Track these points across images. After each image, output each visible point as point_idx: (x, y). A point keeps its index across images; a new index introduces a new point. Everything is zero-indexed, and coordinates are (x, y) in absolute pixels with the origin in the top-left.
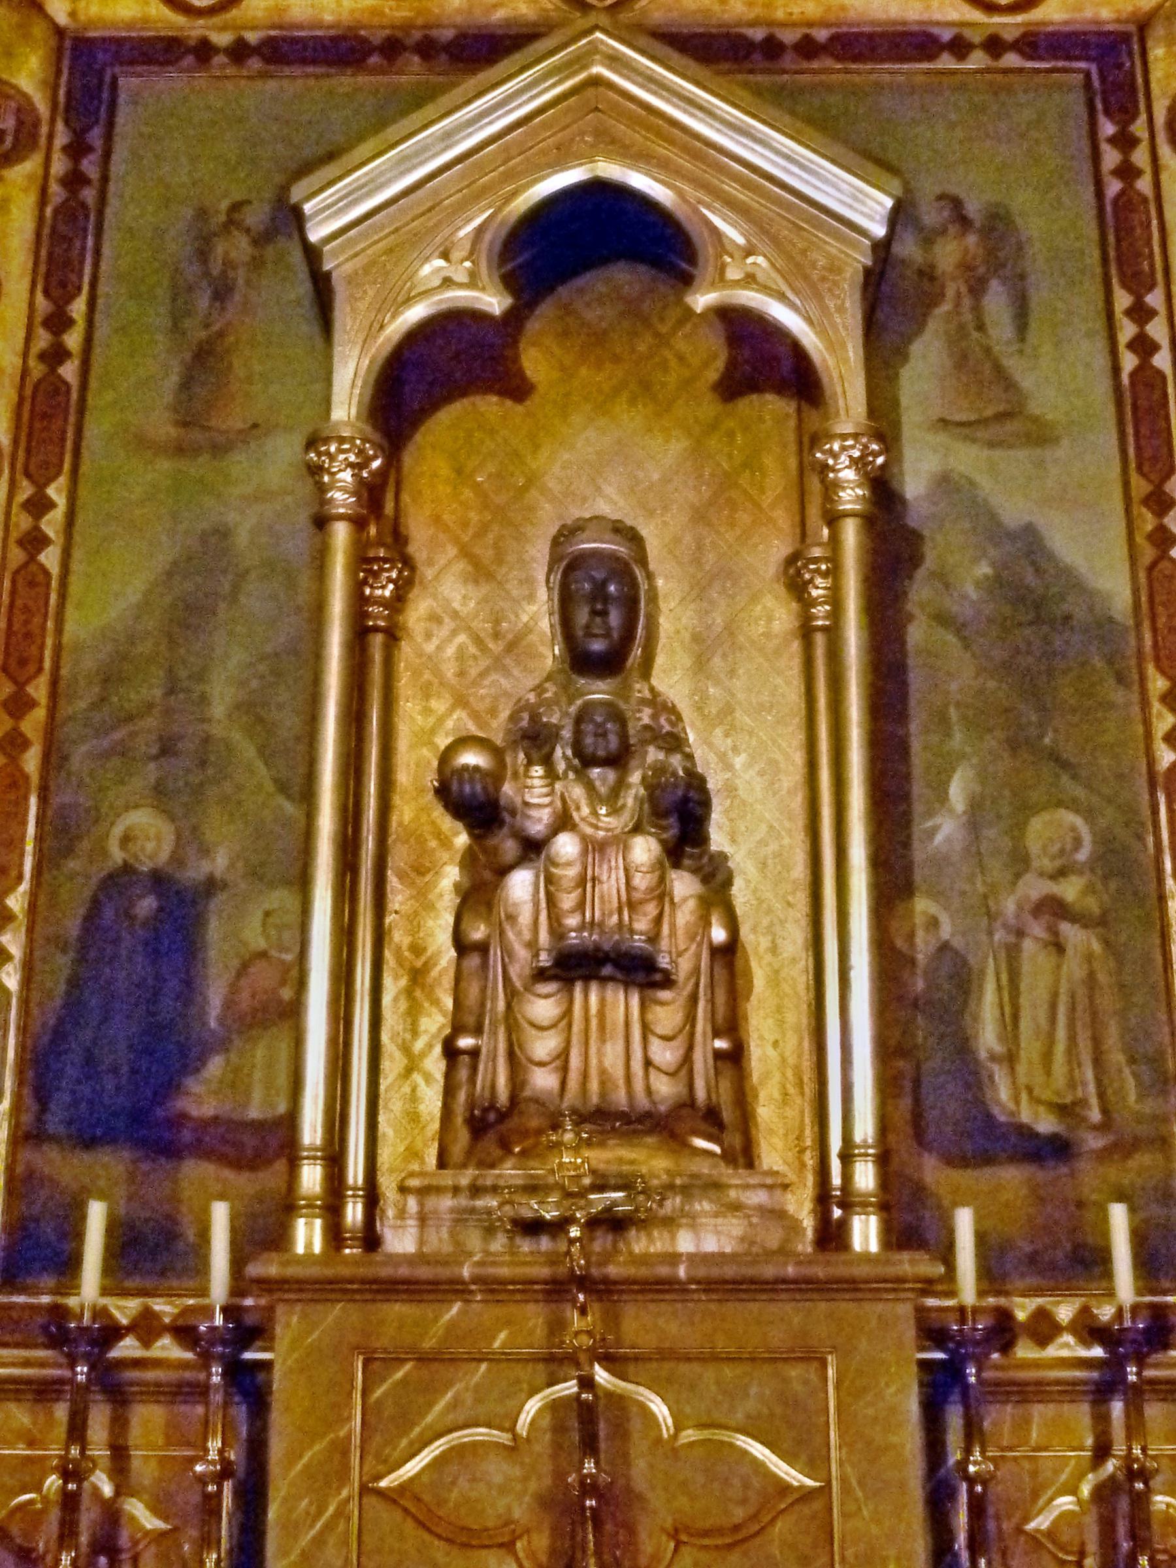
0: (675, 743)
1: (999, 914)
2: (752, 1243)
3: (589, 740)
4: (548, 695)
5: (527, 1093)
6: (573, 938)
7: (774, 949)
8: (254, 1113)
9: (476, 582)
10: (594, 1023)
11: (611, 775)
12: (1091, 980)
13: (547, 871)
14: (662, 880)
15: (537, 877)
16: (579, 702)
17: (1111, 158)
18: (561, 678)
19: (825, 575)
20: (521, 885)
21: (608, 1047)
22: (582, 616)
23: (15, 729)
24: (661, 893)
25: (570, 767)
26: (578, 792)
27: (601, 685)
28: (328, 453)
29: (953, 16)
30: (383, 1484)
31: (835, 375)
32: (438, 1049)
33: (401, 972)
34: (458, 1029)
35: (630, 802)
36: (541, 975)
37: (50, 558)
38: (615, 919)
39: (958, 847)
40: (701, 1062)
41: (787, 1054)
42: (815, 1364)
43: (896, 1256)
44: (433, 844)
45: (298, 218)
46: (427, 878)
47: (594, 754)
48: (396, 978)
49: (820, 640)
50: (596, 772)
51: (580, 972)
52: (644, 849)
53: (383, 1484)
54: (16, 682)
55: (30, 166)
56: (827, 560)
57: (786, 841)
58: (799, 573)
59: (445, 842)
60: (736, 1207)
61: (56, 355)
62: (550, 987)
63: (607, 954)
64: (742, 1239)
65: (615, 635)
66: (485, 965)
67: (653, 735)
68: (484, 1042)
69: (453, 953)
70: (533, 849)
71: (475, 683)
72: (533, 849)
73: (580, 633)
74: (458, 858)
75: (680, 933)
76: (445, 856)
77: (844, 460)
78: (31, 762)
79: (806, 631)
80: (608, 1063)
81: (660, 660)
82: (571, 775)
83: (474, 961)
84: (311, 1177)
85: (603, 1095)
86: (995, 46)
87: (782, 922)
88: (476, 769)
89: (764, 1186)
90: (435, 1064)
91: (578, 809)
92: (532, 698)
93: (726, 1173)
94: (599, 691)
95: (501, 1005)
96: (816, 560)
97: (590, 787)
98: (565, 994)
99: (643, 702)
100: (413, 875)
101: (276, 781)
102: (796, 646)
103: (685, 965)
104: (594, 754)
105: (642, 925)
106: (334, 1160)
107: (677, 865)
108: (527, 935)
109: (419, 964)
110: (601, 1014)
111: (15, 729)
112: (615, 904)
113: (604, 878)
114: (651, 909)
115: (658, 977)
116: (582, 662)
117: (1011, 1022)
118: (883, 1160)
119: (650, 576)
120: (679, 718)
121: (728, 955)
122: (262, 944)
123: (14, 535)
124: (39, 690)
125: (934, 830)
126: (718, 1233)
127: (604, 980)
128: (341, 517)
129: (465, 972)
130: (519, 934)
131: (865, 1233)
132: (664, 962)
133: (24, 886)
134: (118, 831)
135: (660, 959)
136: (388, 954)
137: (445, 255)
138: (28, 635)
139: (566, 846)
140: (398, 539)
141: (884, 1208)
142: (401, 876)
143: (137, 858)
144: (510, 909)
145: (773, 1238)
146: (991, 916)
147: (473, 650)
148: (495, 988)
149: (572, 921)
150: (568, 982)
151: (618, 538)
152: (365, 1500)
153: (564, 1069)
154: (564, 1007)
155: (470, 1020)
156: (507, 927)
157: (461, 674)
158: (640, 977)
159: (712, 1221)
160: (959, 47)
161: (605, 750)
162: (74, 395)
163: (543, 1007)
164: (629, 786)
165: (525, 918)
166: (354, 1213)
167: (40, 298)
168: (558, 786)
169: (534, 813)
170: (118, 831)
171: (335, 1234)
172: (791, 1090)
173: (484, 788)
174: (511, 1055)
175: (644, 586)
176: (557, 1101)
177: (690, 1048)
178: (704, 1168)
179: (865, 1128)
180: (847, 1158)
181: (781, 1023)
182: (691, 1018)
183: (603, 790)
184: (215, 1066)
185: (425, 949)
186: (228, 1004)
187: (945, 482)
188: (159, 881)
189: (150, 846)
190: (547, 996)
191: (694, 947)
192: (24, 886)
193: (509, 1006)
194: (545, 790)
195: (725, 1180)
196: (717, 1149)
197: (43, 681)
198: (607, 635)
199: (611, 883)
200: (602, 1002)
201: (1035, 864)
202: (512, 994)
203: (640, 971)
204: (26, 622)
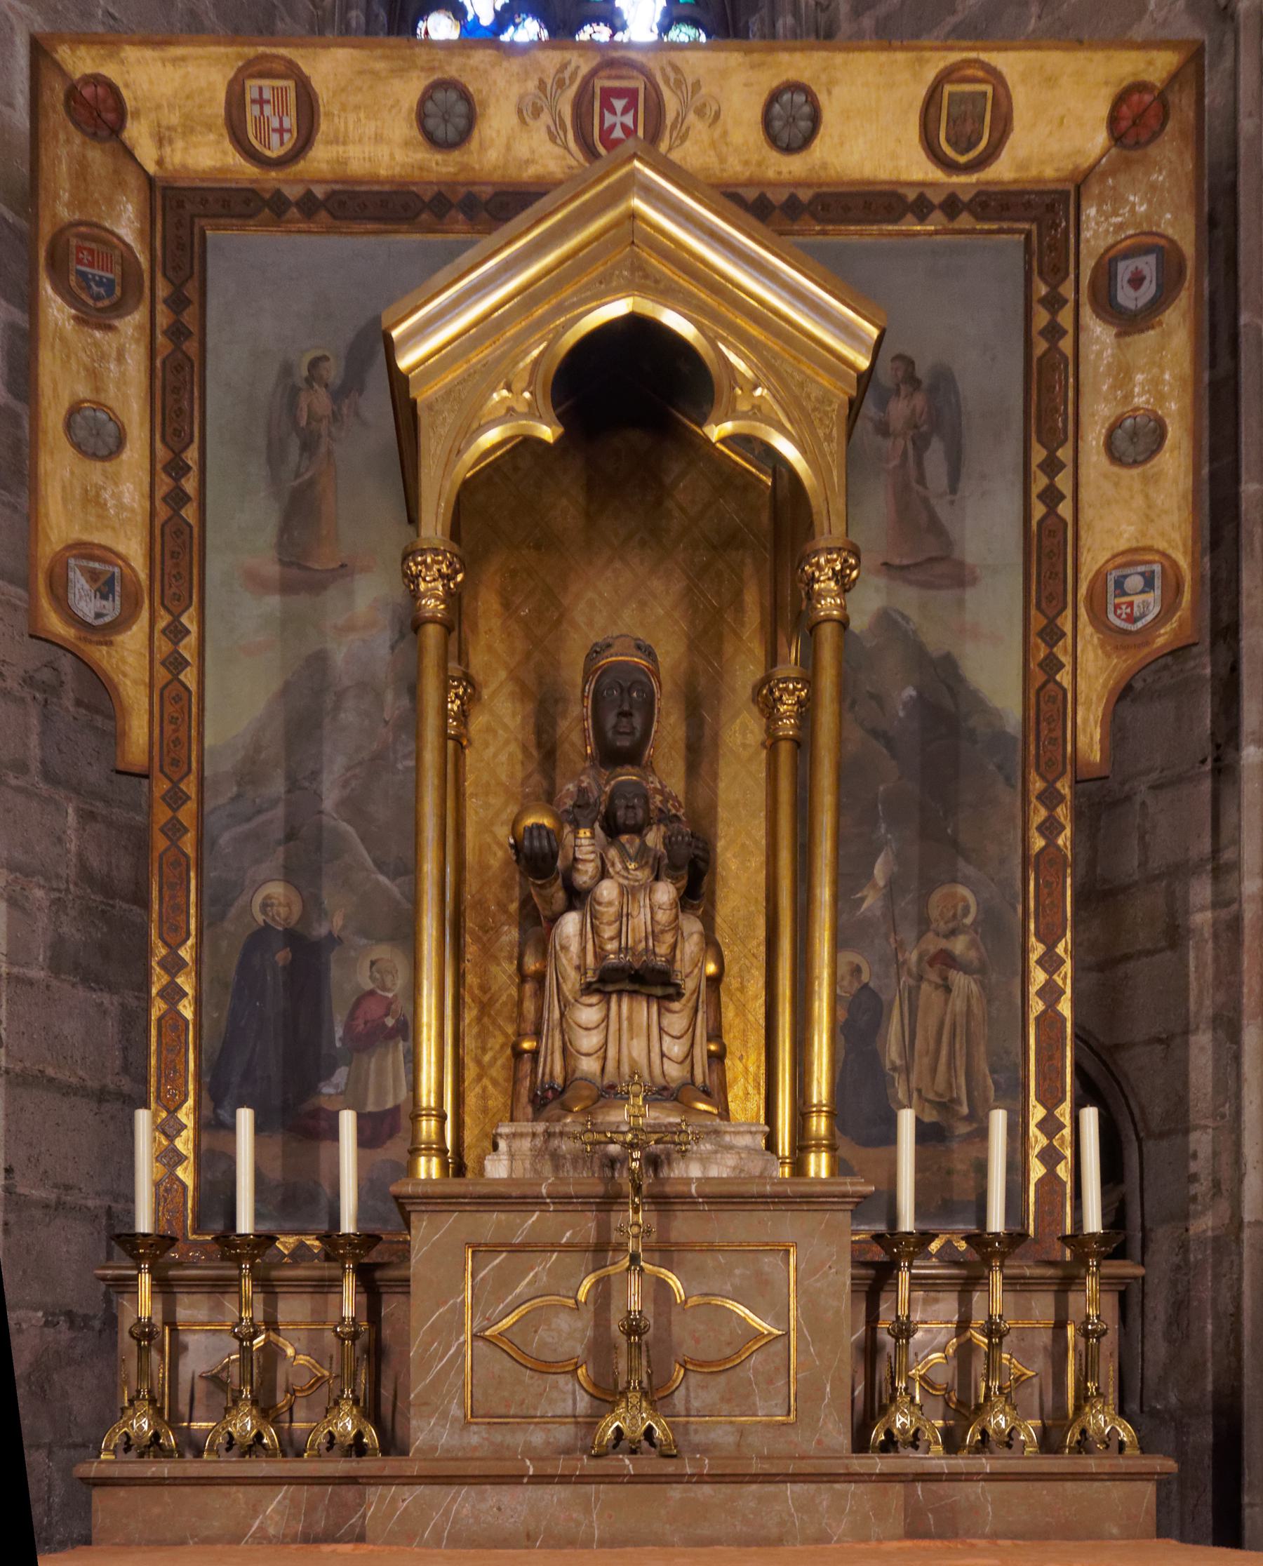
3: (620, 813)
5: (578, 1075)
10: (625, 1024)
14: (677, 917)
15: (584, 916)
20: (570, 923)
23: (174, 818)
26: (613, 853)
30: (487, 1333)
36: (588, 989)
37: (189, 677)
50: (624, 838)
51: (618, 987)
53: (487, 1333)
54: (170, 780)
62: (594, 999)
65: (638, 734)
70: (577, 897)
72: (577, 897)
75: (687, 957)
78: (188, 844)
89: (751, 1133)
91: (613, 865)
94: (628, 775)
95: (557, 1014)
98: (603, 1006)
105: (663, 949)
108: (576, 961)
110: (630, 1019)
111: (174, 818)
114: (669, 938)
124: (189, 786)
127: (632, 993)
138: (177, 742)
144: (564, 942)
150: (606, 996)
151: (639, 654)
153: (605, 1058)
154: (604, 1013)
156: (562, 955)
158: (659, 991)
163: (588, 1014)
165: (574, 947)
174: (564, 1050)
176: (599, 1080)
179: (820, 1090)
190: (591, 1005)
193: (562, 1015)
196: (715, 1111)
197: (192, 777)
202: (565, 1005)
204: (176, 731)
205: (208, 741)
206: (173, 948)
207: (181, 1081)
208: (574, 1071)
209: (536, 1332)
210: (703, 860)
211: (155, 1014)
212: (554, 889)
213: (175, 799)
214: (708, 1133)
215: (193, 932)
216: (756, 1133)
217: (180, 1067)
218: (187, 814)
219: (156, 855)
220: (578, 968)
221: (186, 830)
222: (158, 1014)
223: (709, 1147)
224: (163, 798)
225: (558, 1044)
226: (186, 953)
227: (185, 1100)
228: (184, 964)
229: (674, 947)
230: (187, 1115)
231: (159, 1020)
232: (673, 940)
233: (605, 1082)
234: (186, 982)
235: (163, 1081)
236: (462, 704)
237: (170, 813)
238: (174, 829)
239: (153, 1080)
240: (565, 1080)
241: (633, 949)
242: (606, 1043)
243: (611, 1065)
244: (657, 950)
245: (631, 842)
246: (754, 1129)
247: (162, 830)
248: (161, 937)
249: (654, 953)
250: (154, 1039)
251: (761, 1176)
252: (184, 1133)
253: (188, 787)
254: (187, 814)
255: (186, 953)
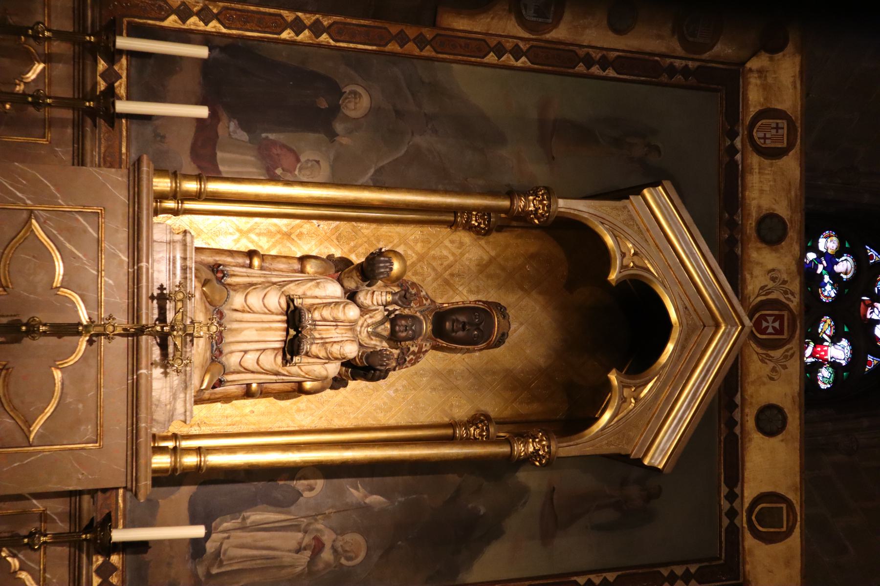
0: (401, 362)
1: (316, 520)
2: (157, 406)
4: (424, 302)
6: (308, 316)
7: (299, 410)
8: (219, 155)
9: (478, 265)
11: (386, 334)
12: (282, 567)
13: (342, 302)
14: (336, 359)
15: (338, 298)
16: (422, 318)
17: (679, 570)
18: (432, 307)
19: (481, 435)
20: (334, 290)
21: (255, 332)
22: (462, 318)
23: (409, 40)
24: (329, 359)
25: (390, 313)
26: (379, 317)
27: (430, 328)
28: (543, 200)
29: (746, 494)
30: (34, 221)
31: (578, 441)
32: (252, 248)
33: (289, 227)
34: (263, 257)
35: (373, 342)
36: (290, 300)
37: (491, 58)
38: (317, 336)
39: (348, 500)
40: (247, 377)
41: (248, 418)
42: (95, 438)
43: (150, 475)
44: (352, 244)
45: (654, 185)
46: (335, 241)
47: (397, 325)
48: (287, 225)
49: (450, 432)
50: (388, 325)
52: (351, 351)
53: (34, 221)
54: (432, 40)
55: (679, 51)
56: (488, 436)
57: (352, 416)
58: (482, 421)
59: (352, 250)
60: (175, 397)
61: (589, 62)
62: (284, 306)
63: (300, 332)
64: (159, 401)
65: (454, 334)
66: (295, 271)
67: (405, 352)
68: (256, 271)
69: (299, 255)
70: (352, 296)
71: (429, 264)
72: (352, 296)
73: (454, 317)
74: (344, 256)
76: (345, 250)
77: (538, 447)
79: (452, 425)
80: (245, 332)
81: (440, 354)
82: (386, 313)
83: (297, 266)
84: (191, 186)
85: (231, 330)
86: (732, 514)
87: (312, 415)
88: (391, 269)
89: (185, 412)
90: (245, 245)
91: (371, 317)
92: (423, 293)
93: (191, 393)
94: (427, 327)
95: (275, 280)
96: (488, 430)
97: (382, 323)
99: (421, 348)
100: (337, 234)
101: (383, 167)
102: (446, 420)
103: (294, 369)
104: (397, 325)
105: (315, 349)
106: (198, 196)
107: (343, 364)
108: (309, 293)
109: (293, 236)
110: (270, 329)
112: (324, 336)
113: (338, 331)
114: (322, 354)
115: (289, 357)
116: (441, 317)
117: (259, 527)
118: (198, 468)
119: (481, 350)
120: (412, 365)
121: (299, 390)
122: (303, 159)
123: (503, 40)
124: (428, 52)
125: (357, 489)
126: (162, 388)
128: (512, 203)
129: (291, 261)
130: (310, 288)
131: (162, 461)
132: (296, 359)
133: (332, 43)
134: (360, 90)
135: (297, 358)
136: (298, 221)
137: (635, 254)
139: (353, 312)
140: (500, 229)
141: (174, 469)
142: (337, 228)
143: (346, 98)
144: (322, 284)
145: (160, 415)
146: (314, 517)
147: (446, 263)
148: (282, 276)
149: (316, 315)
152: (25, 212)
153: (243, 311)
154: (273, 310)
155: (266, 265)
156: (314, 283)
157: (434, 258)
159: (168, 385)
160: (732, 497)
161: (397, 330)
162: (571, 71)
163: (275, 301)
164: (381, 342)
165: (317, 292)
166: (171, 204)
167: (618, 53)
168: (382, 308)
169: (369, 295)
170: (360, 90)
171: (161, 196)
172: (229, 420)
173: (382, 273)
174: (251, 285)
175: (476, 348)
177: (253, 372)
178: (196, 381)
179: (215, 460)
180: (199, 451)
181: (263, 414)
182: (267, 372)
183: (379, 330)
184: (243, 136)
185: (300, 240)
186: (274, 143)
187: (523, 491)
188: (334, 110)
189: (352, 105)
190: (279, 303)
191: (303, 374)
192: (332, 43)
194: (380, 302)
195: (188, 392)
197: (433, 54)
198: (453, 331)
199: (334, 334)
200: (276, 329)
201: (340, 538)
203: (292, 348)
204: (461, 46)
205: (454, 65)
206: (328, 30)
207: (239, 26)
208: (235, 290)
209: (34, 257)
210: (374, 375)
211: (285, 13)
212: (356, 278)
213: (421, 42)
214: (185, 382)
215: (338, 44)
216: (185, 415)
217: (248, 26)
218: (411, 48)
219: (387, 26)
220: (304, 294)
221: (402, 46)
222: (285, 15)
223: (176, 382)
224: (421, 34)
225: (254, 280)
226: (324, 38)
227: (225, 27)
228: (318, 37)
229: (318, 358)
230: (215, 27)
231: (280, 15)
232: (321, 356)
233: (226, 312)
234: (305, 36)
235: (239, 13)
236: (475, 227)
237: (412, 37)
238: (402, 39)
239: (239, 6)
240: (229, 285)
241: (315, 330)
242: (254, 312)
243: (238, 315)
244: (314, 346)
245: (385, 330)
246: (188, 413)
247: (402, 31)
248: (335, 23)
249: (312, 344)
250: (267, 10)
251: (152, 420)
252: (202, 23)
253: (428, 51)
254: (411, 48)
255: (324, 38)
